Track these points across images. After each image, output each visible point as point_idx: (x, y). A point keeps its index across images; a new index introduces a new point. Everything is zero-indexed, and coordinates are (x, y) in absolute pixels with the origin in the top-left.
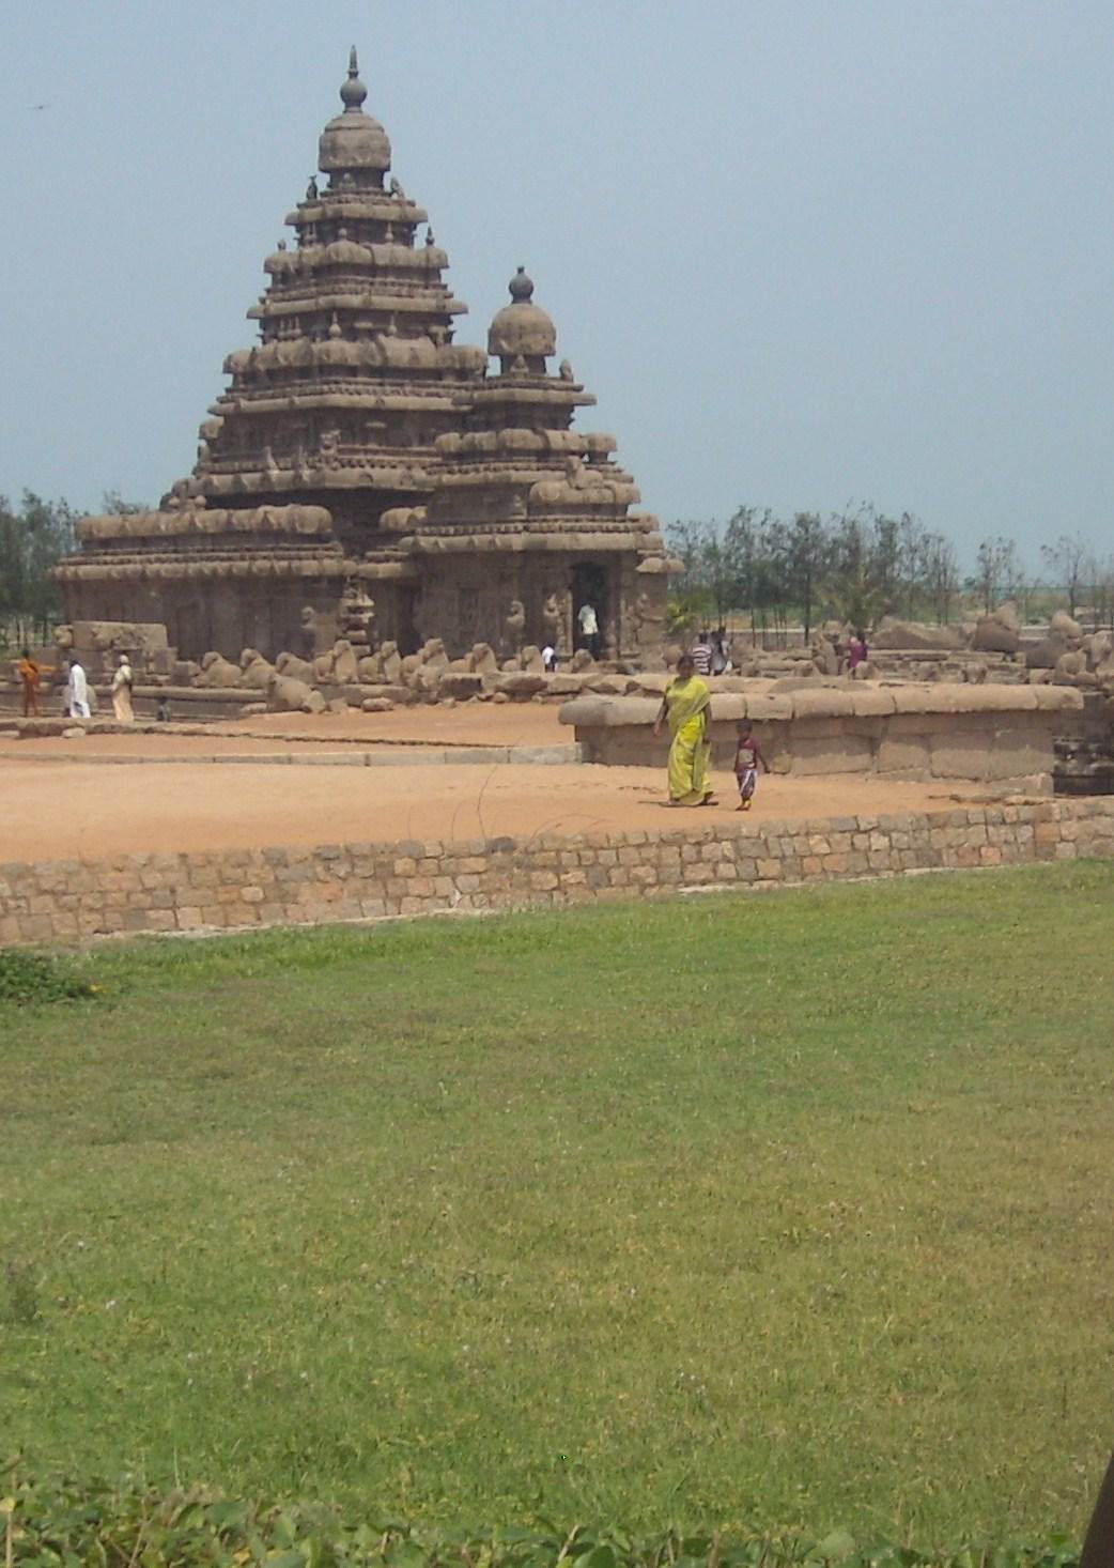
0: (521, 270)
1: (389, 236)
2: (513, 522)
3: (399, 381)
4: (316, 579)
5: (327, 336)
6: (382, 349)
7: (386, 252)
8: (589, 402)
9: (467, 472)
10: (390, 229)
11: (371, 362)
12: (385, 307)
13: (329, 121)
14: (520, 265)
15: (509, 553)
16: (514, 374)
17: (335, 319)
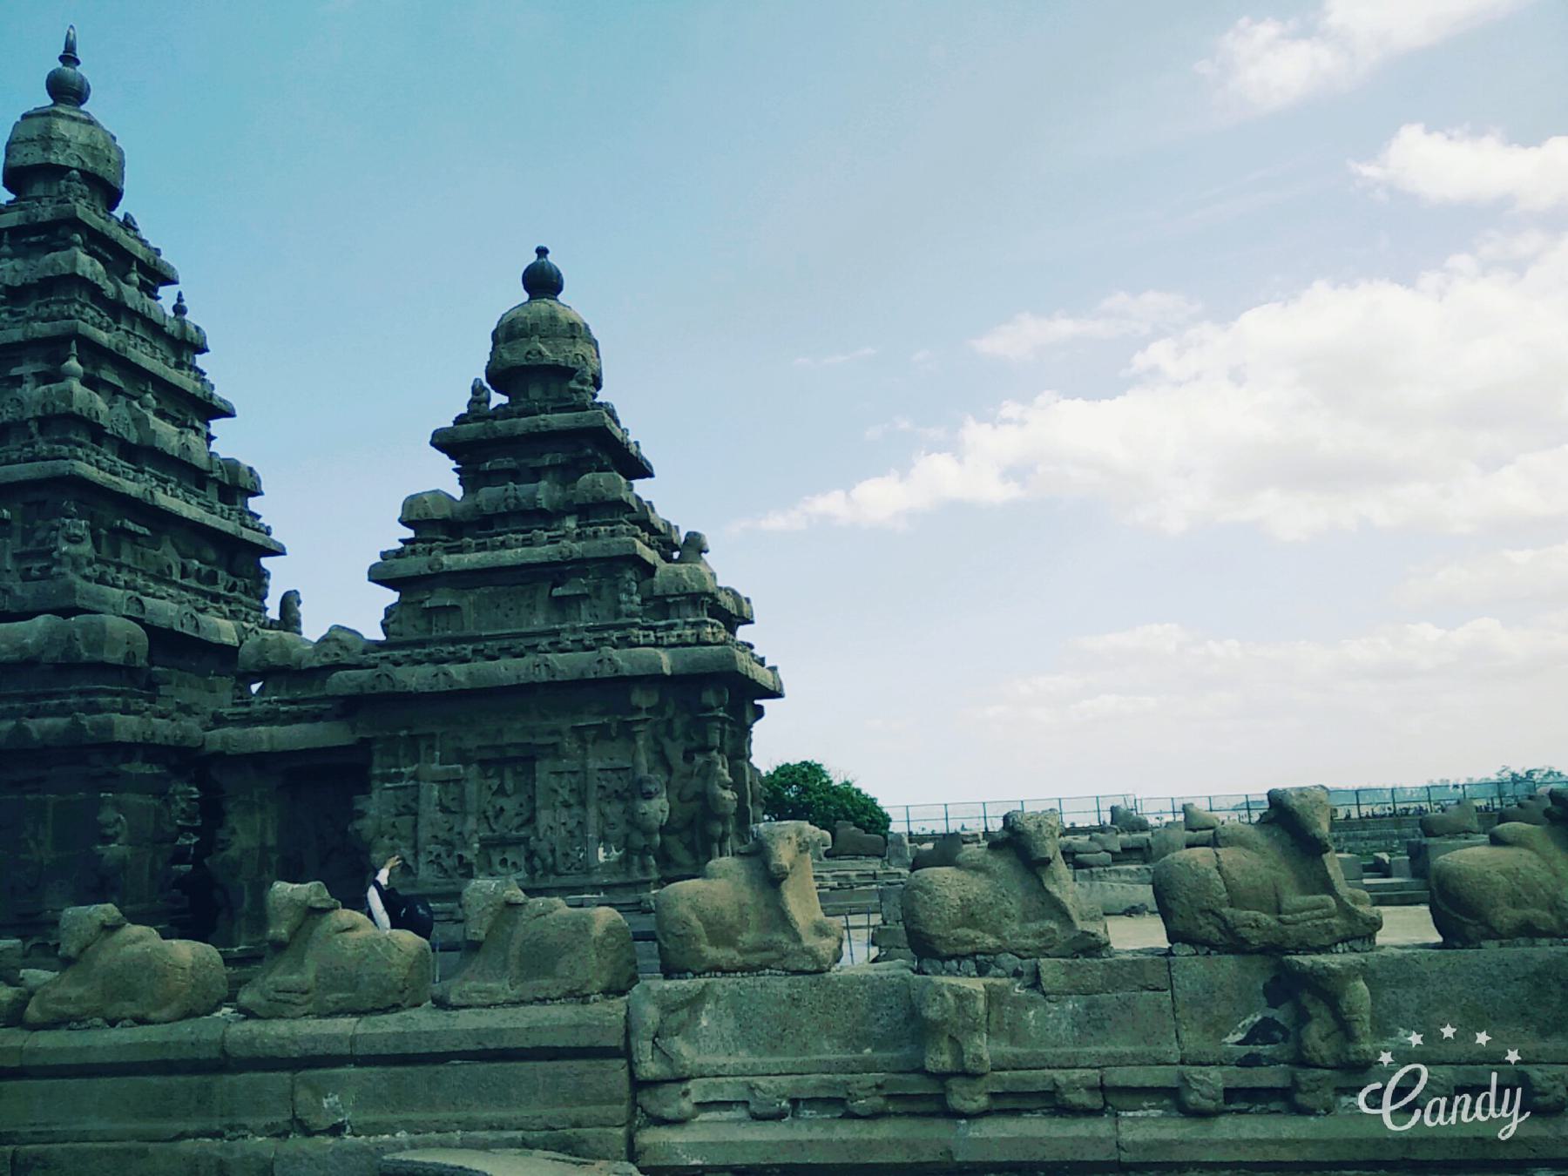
0: (542, 252)
1: (134, 277)
2: (634, 625)
3: (165, 476)
4: (129, 750)
5: (45, 378)
6: (140, 421)
7: (132, 295)
8: (644, 471)
9: (503, 545)
10: (135, 264)
11: (125, 436)
12: (143, 365)
13: (32, 109)
14: (543, 244)
15: (654, 680)
16: (576, 391)
17: (75, 352)
